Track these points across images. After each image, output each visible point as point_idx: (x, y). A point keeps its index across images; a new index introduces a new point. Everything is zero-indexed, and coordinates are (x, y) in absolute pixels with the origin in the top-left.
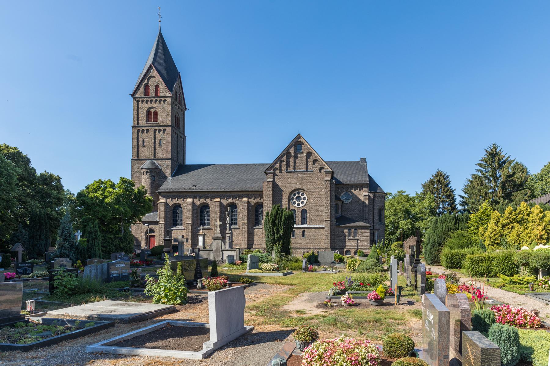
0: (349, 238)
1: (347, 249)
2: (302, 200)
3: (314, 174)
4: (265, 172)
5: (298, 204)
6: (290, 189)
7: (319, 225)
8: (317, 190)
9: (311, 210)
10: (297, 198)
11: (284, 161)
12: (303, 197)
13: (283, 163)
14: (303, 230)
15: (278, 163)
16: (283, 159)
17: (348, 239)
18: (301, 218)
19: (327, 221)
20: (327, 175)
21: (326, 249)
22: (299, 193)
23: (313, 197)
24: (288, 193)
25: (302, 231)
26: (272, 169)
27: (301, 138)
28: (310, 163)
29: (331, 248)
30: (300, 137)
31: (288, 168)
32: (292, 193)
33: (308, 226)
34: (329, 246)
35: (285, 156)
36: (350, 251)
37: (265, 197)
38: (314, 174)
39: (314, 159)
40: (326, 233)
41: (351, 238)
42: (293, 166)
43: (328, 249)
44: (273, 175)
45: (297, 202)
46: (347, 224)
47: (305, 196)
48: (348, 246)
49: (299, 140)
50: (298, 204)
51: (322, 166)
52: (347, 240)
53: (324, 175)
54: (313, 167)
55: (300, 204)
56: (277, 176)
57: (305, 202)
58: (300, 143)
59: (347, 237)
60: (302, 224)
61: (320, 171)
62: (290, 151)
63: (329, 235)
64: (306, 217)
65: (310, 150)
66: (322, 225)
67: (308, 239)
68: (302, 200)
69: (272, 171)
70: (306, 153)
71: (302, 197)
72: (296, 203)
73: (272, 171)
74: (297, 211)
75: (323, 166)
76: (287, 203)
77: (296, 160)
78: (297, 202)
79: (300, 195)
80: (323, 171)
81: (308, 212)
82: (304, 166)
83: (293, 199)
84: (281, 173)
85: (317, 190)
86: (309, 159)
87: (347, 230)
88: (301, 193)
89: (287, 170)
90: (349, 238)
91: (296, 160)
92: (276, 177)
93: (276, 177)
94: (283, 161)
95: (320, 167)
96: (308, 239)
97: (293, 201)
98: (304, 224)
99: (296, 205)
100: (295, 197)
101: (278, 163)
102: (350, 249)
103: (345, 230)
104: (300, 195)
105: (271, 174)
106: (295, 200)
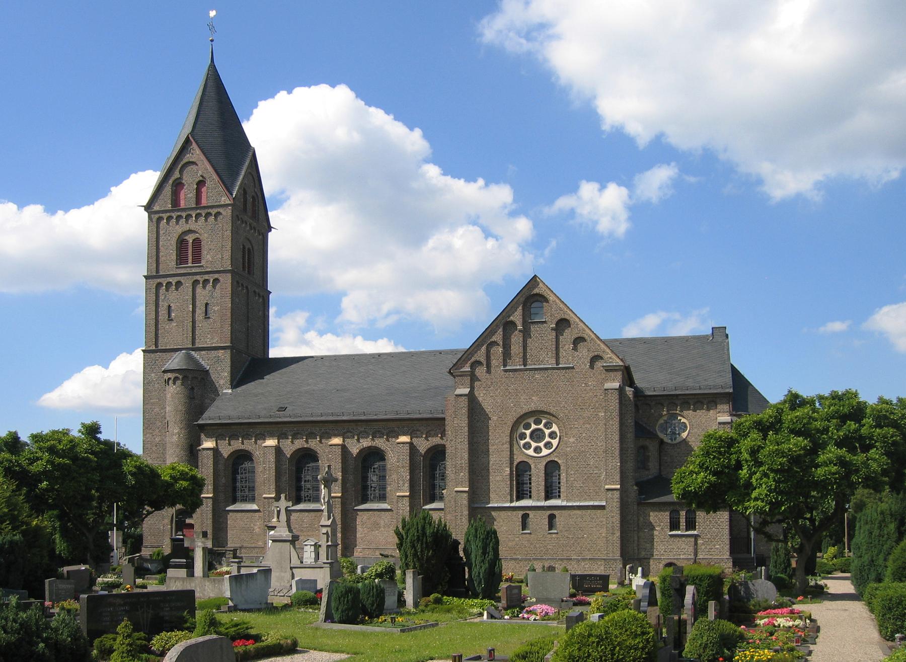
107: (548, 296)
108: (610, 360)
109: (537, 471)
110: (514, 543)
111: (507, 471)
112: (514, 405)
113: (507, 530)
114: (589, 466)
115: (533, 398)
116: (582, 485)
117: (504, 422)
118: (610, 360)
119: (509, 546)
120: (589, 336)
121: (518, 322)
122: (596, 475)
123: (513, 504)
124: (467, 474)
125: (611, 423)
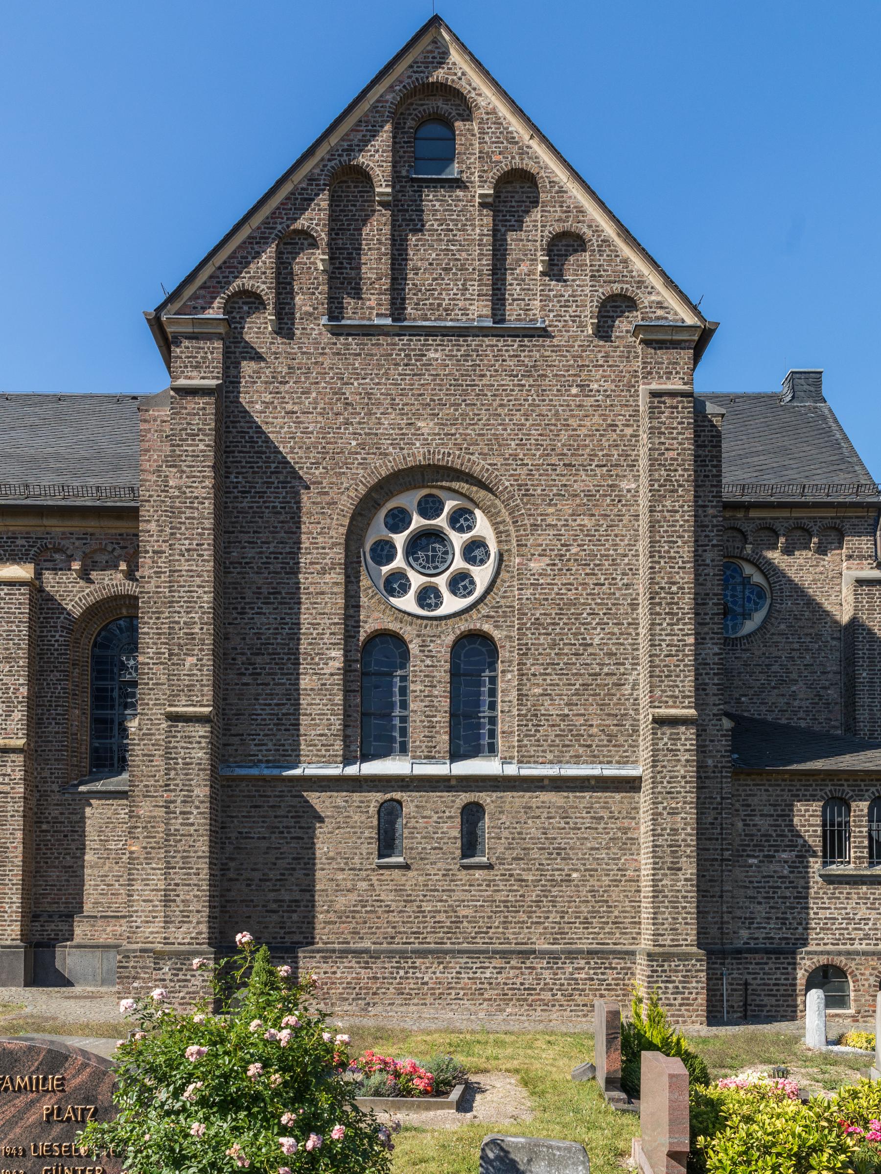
0: (835, 869)
1: (823, 960)
2: (459, 563)
3: (556, 349)
4: (156, 324)
5: (429, 597)
6: (363, 465)
7: (594, 759)
8: (583, 482)
9: (529, 638)
10: (413, 546)
11: (314, 245)
12: (467, 536)
13: (302, 258)
14: (465, 798)
15: (267, 257)
16: (302, 223)
17: (829, 879)
18: (445, 704)
19: (673, 722)
20: (664, 356)
21: (667, 957)
22: (431, 508)
23: (546, 538)
24: (347, 503)
25: (455, 812)
26: (218, 303)
27: (455, 56)
28: (524, 268)
29: (710, 953)
30: (446, 54)
31: (349, 302)
32: (378, 506)
33: (511, 770)
34: (689, 934)
35: (323, 201)
36: (841, 973)
37: (153, 526)
38: (556, 349)
39: (558, 228)
40: (667, 822)
41: (850, 869)
42: (386, 283)
43: (685, 957)
44: (227, 354)
45: (416, 580)
46: (810, 760)
47: (482, 527)
48: (828, 938)
49: (439, 75)
50: (429, 597)
51: (616, 288)
52: (816, 882)
53: (638, 364)
54: (545, 299)
55: (438, 595)
56: (258, 357)
57: (482, 575)
58: (440, 105)
59: (815, 865)
60: (455, 756)
61: (603, 331)
62: (362, 159)
63: (692, 841)
64: (486, 699)
65: (523, 152)
66: (624, 762)
67: (508, 876)
68: (459, 563)
69: (215, 312)
70: (493, 175)
71: (458, 540)
72: (405, 588)
73: (215, 312)
74: (414, 648)
75: (630, 289)
76: (337, 576)
77: (413, 239)
78: (416, 580)
79: (442, 521)
80: (623, 326)
81: (503, 654)
82: (474, 288)
83: (385, 552)
84: (290, 335)
85: (583, 482)
86: (511, 236)
87: (816, 807)
88: (449, 505)
89: (335, 311)
90: (835, 869)
91: (413, 239)
92: (248, 367)
93: (248, 367)
94: (307, 239)
95: (604, 291)
96: (508, 876)
97: (385, 569)
98: (473, 753)
99: (408, 602)
100: (400, 540)
101: (267, 257)
102: (840, 961)
103: (799, 806)
104: (442, 521)
105: (208, 337)
106: (399, 562)
107: (473, 95)
108: (660, 313)
109: (428, 662)
110: (353, 897)
111: (334, 659)
112: (362, 446)
113: (331, 854)
114: (590, 650)
115: (420, 424)
116: (566, 711)
117: (327, 498)
118: (660, 313)
119: (337, 907)
120: (597, 231)
121: (376, 169)
122: (610, 680)
123: (352, 770)
124: (208, 661)
125: (668, 503)
